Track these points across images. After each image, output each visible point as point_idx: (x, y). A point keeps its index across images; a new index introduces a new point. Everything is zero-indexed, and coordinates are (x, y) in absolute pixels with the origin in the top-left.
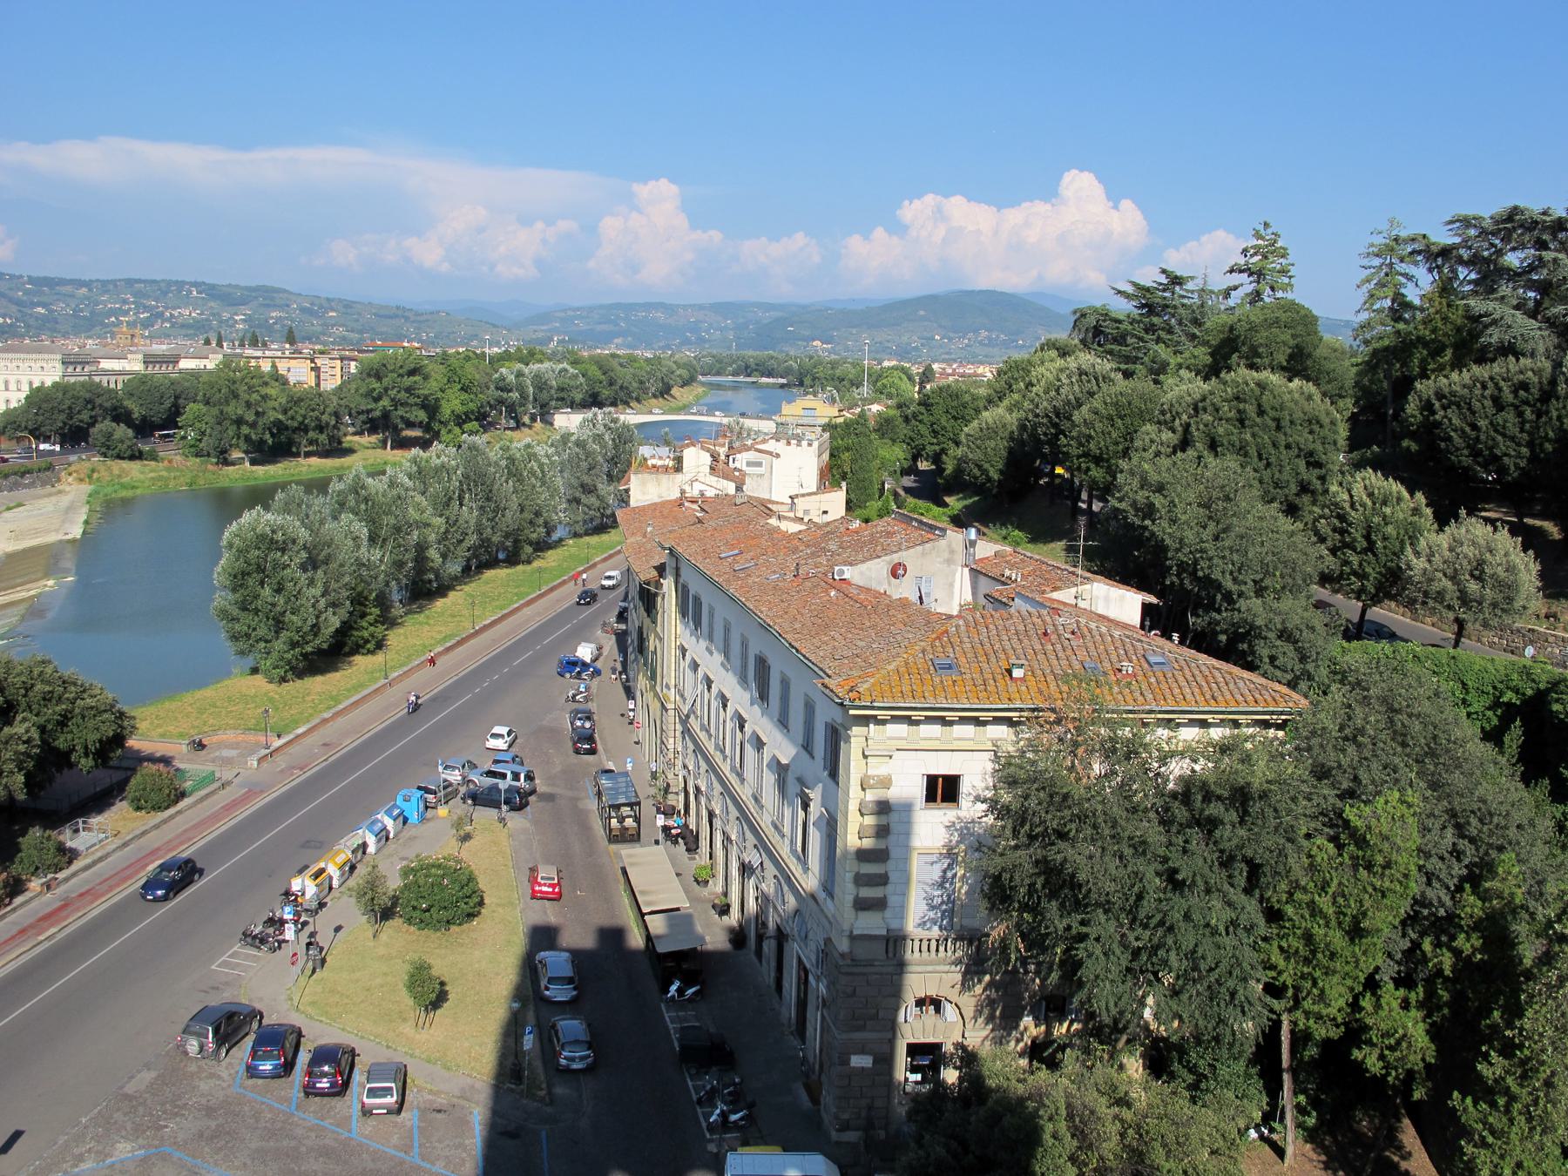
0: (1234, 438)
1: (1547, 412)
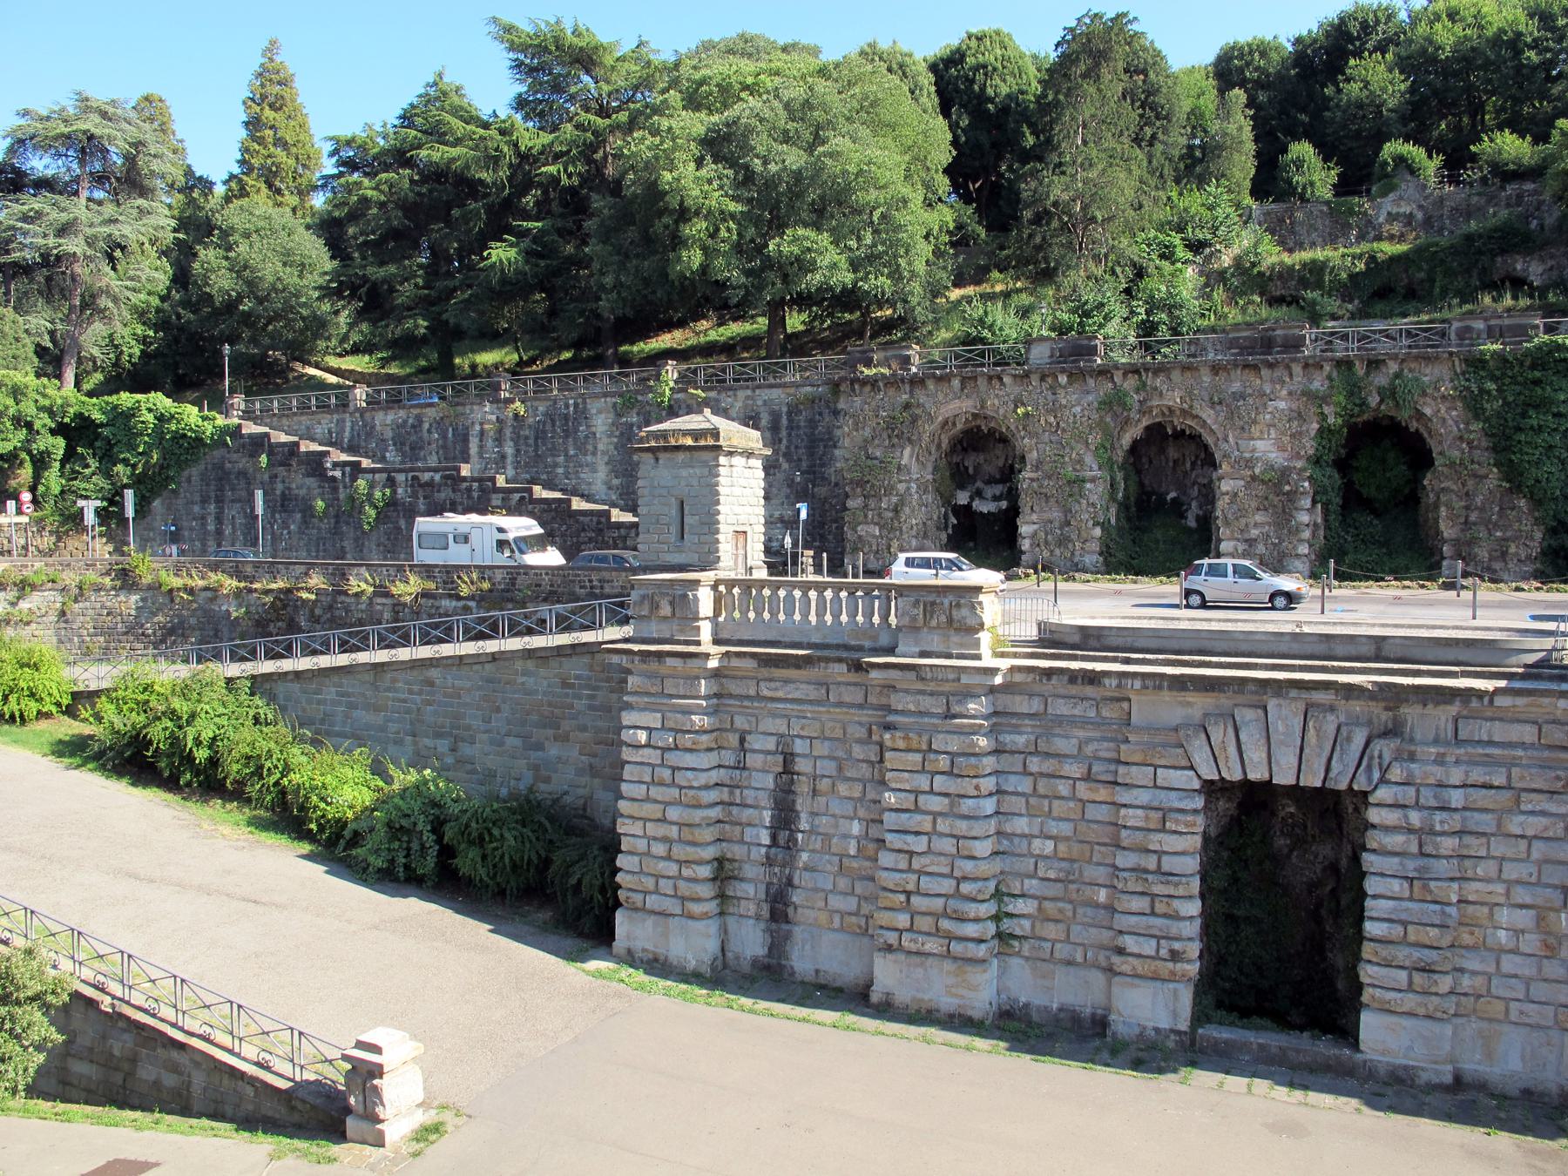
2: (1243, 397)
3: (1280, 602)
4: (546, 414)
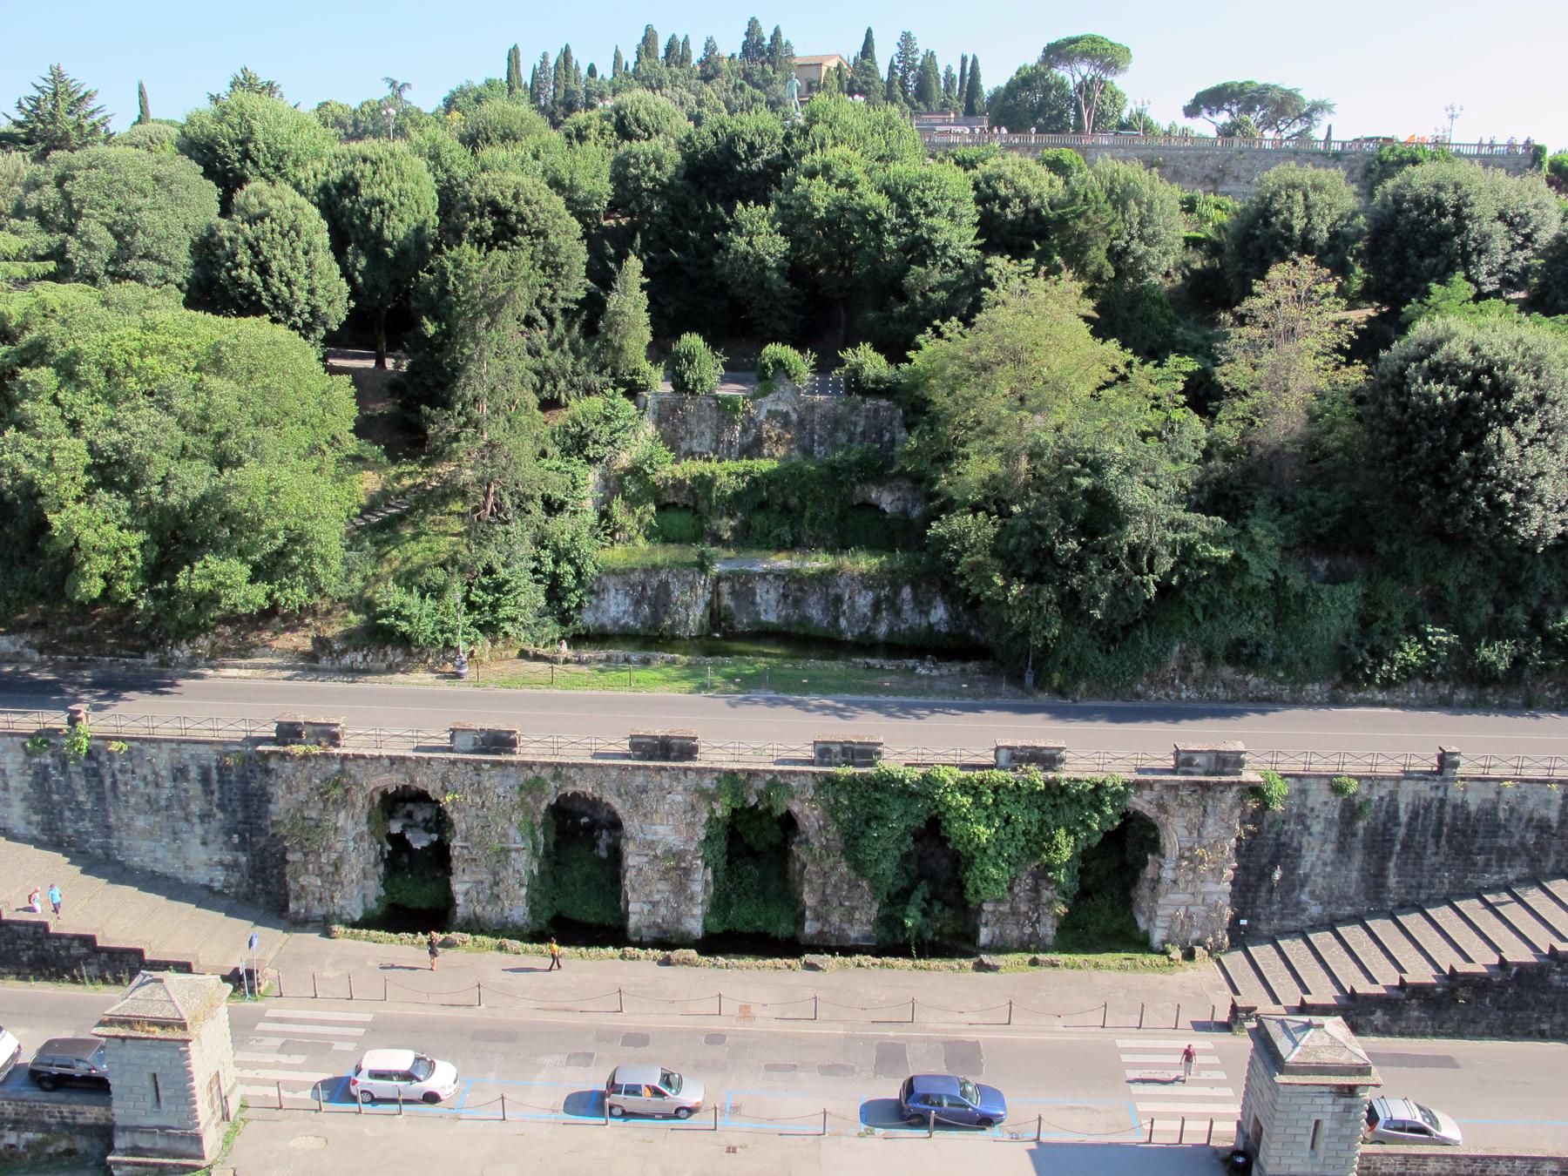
2: (644, 790)
3: (683, 1113)
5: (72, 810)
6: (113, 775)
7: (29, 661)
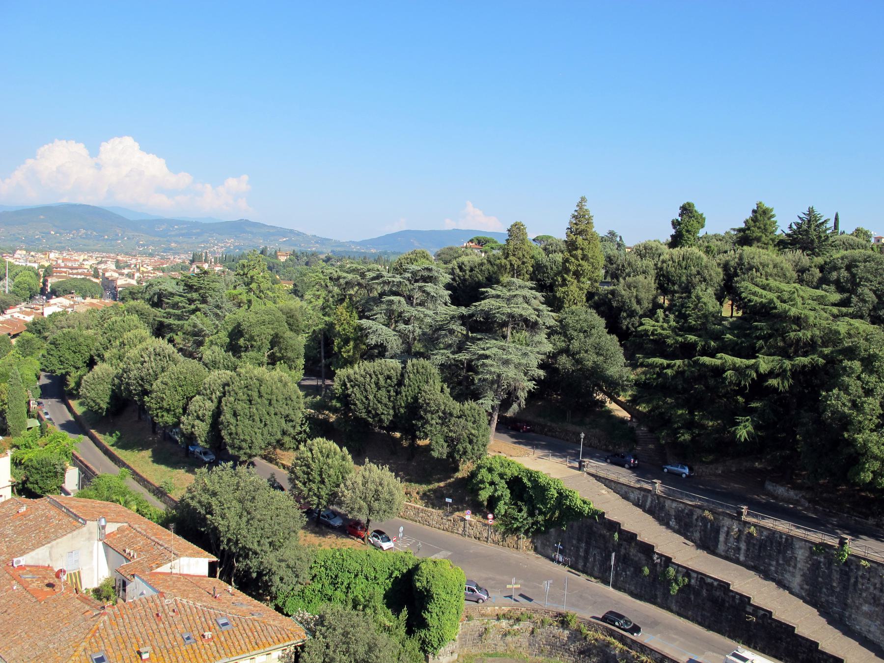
0: (247, 411)
1: (400, 393)
4: (767, 537)
5: (827, 589)
6: (856, 578)
7: (802, 506)
